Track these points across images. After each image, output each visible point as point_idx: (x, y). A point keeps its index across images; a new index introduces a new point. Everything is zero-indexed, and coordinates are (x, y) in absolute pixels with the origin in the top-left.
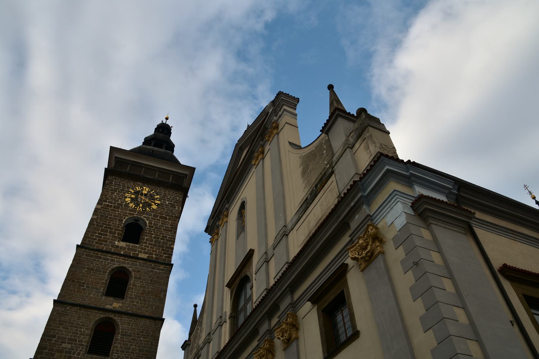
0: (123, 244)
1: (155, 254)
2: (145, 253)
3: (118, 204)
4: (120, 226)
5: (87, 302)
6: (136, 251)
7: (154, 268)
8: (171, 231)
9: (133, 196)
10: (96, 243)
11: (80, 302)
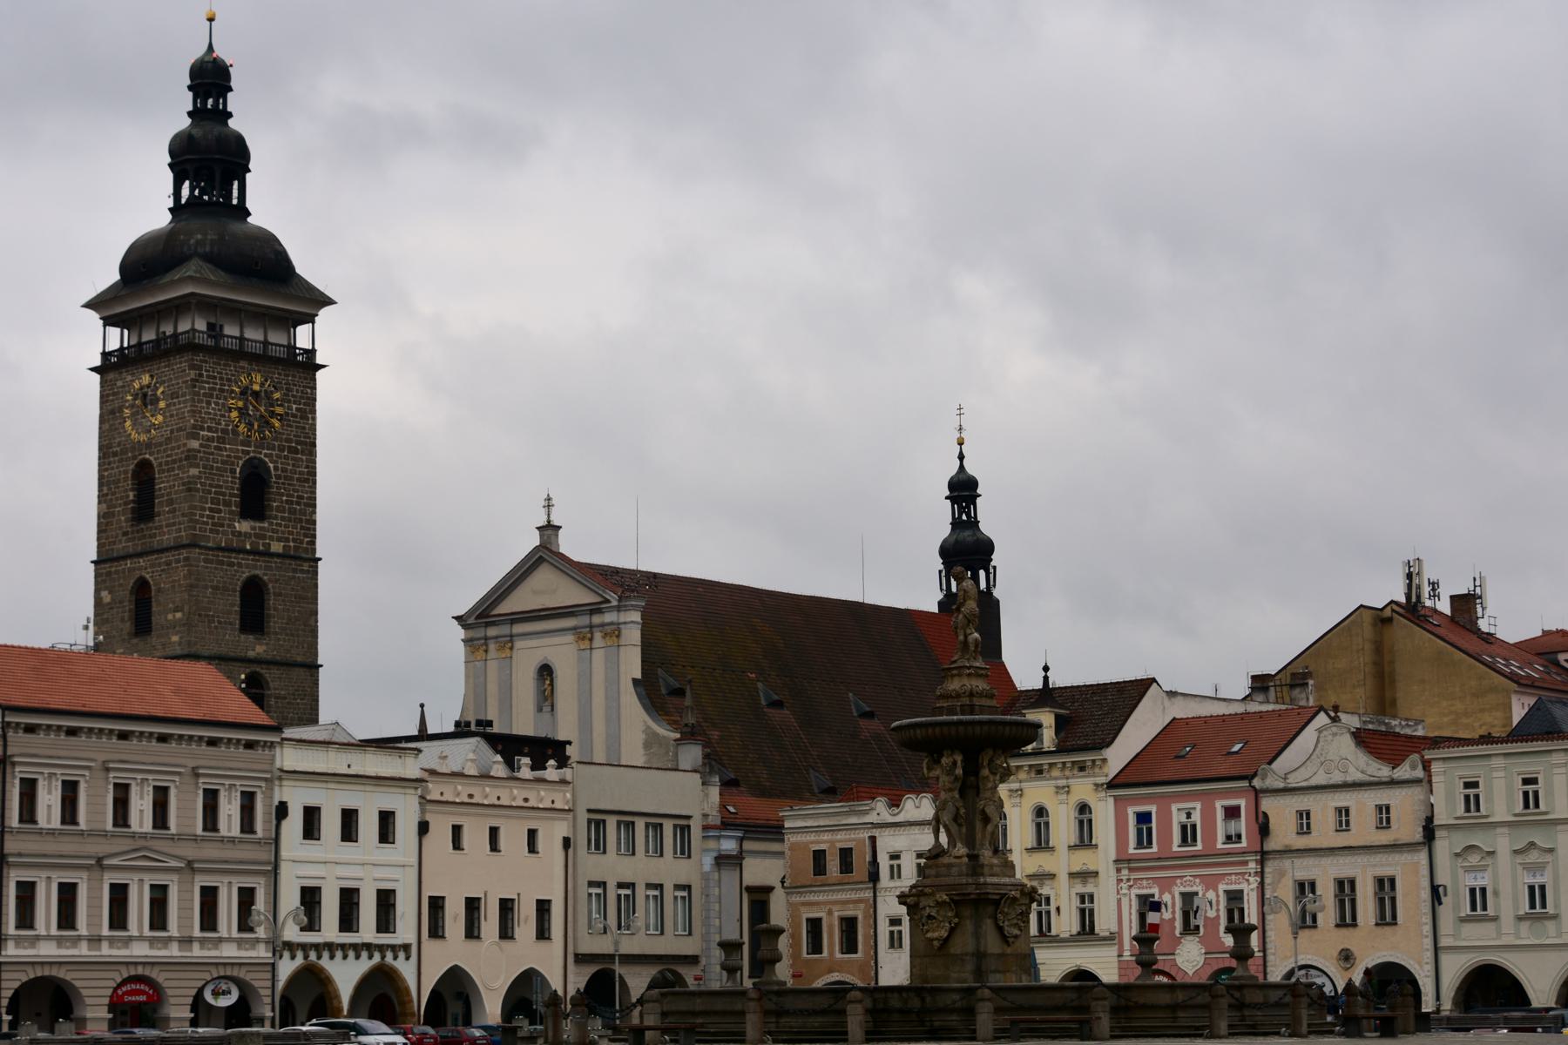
0: (244, 526)
1: (294, 540)
2: (279, 540)
3: (223, 431)
4: (231, 485)
5: (223, 650)
6: (264, 537)
7: (295, 571)
8: (307, 481)
9: (240, 404)
10: (211, 531)
11: (214, 650)
